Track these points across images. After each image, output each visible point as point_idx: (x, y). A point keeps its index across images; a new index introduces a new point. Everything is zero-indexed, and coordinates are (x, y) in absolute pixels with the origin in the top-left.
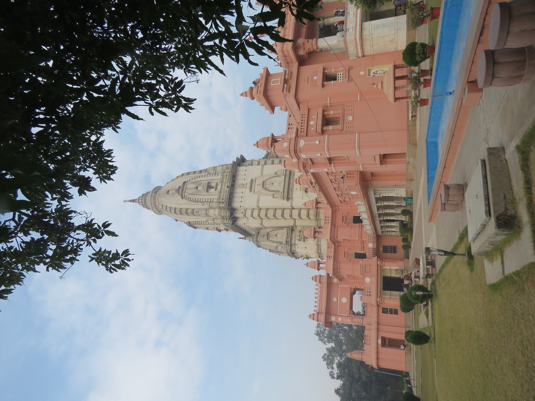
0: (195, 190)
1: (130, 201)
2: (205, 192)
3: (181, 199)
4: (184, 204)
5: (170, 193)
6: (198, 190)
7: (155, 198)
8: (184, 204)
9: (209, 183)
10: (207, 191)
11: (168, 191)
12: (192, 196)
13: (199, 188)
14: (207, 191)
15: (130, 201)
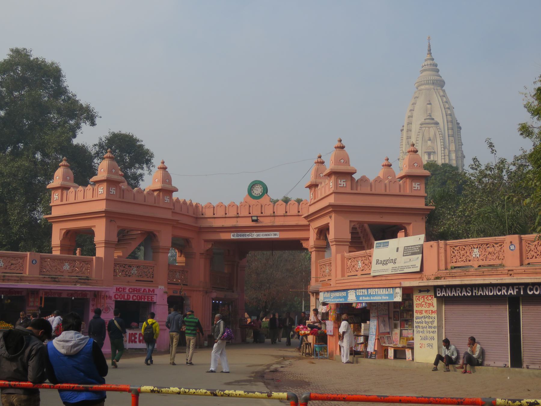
0: (427, 137)
1: (429, 46)
2: (426, 151)
3: (420, 122)
4: (415, 127)
5: (429, 106)
6: (427, 142)
7: (428, 84)
8: (415, 127)
9: (434, 152)
10: (425, 152)
11: (430, 104)
12: (421, 136)
13: (429, 142)
14: (425, 152)
15: (429, 46)
